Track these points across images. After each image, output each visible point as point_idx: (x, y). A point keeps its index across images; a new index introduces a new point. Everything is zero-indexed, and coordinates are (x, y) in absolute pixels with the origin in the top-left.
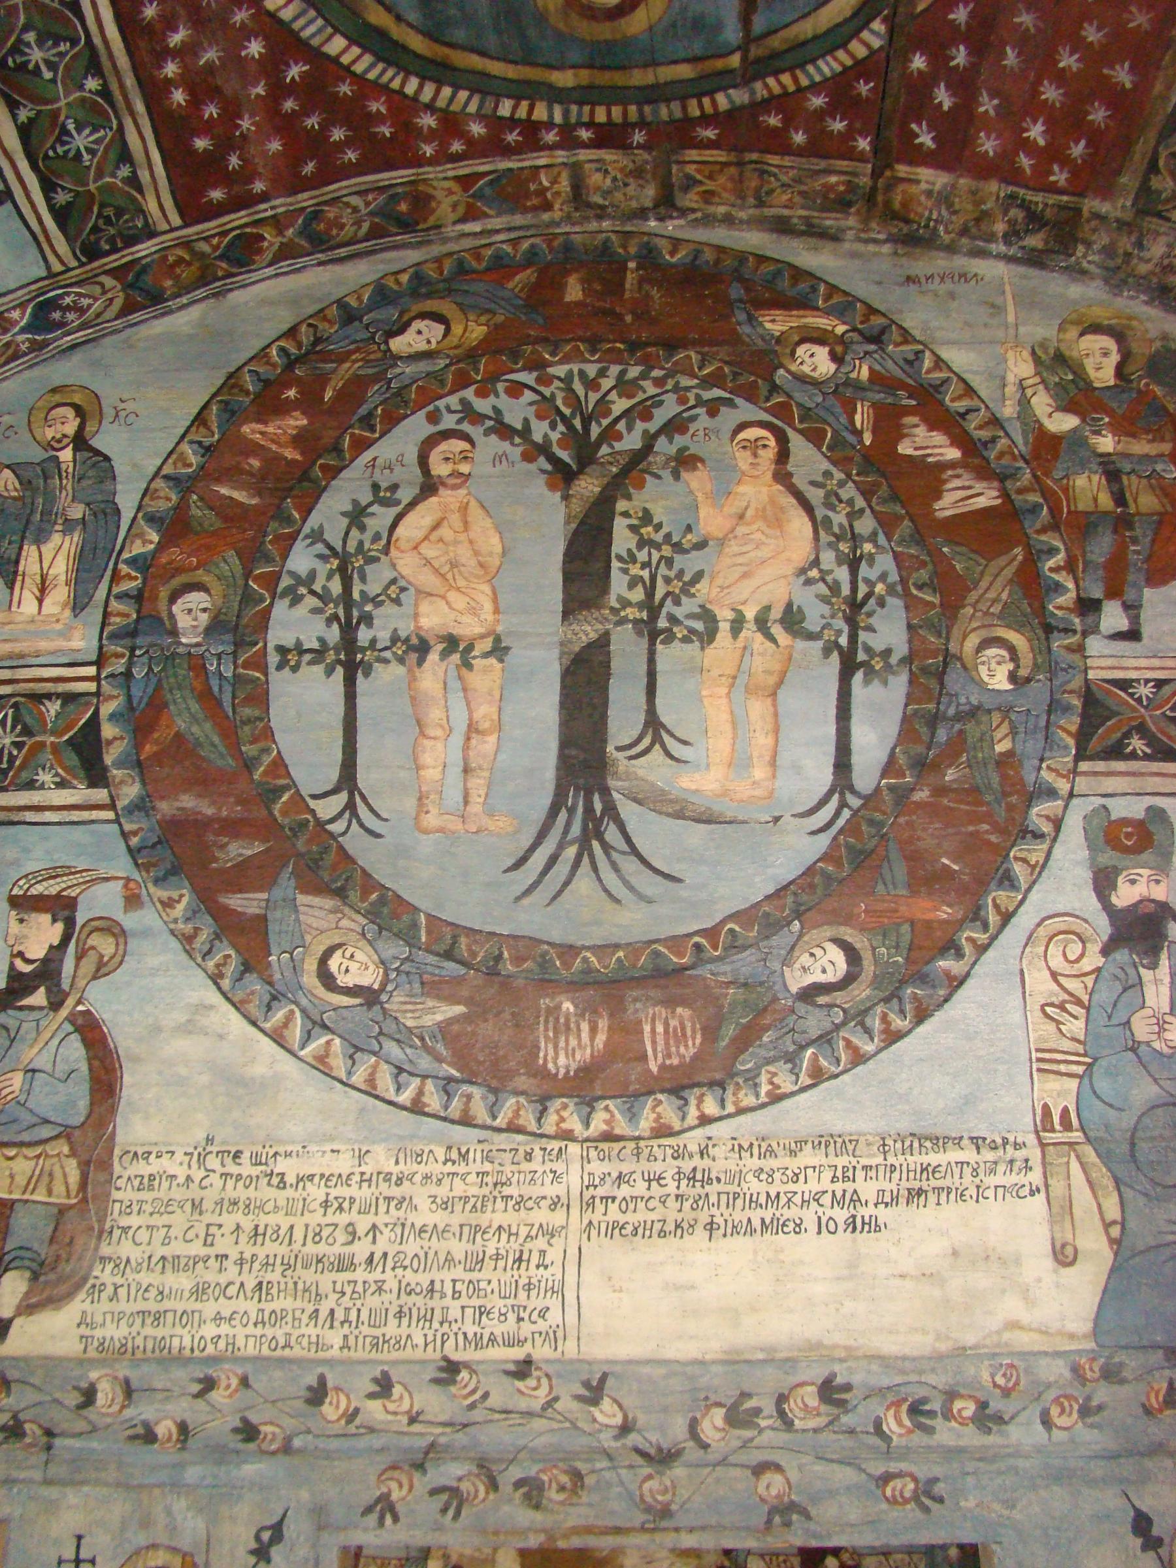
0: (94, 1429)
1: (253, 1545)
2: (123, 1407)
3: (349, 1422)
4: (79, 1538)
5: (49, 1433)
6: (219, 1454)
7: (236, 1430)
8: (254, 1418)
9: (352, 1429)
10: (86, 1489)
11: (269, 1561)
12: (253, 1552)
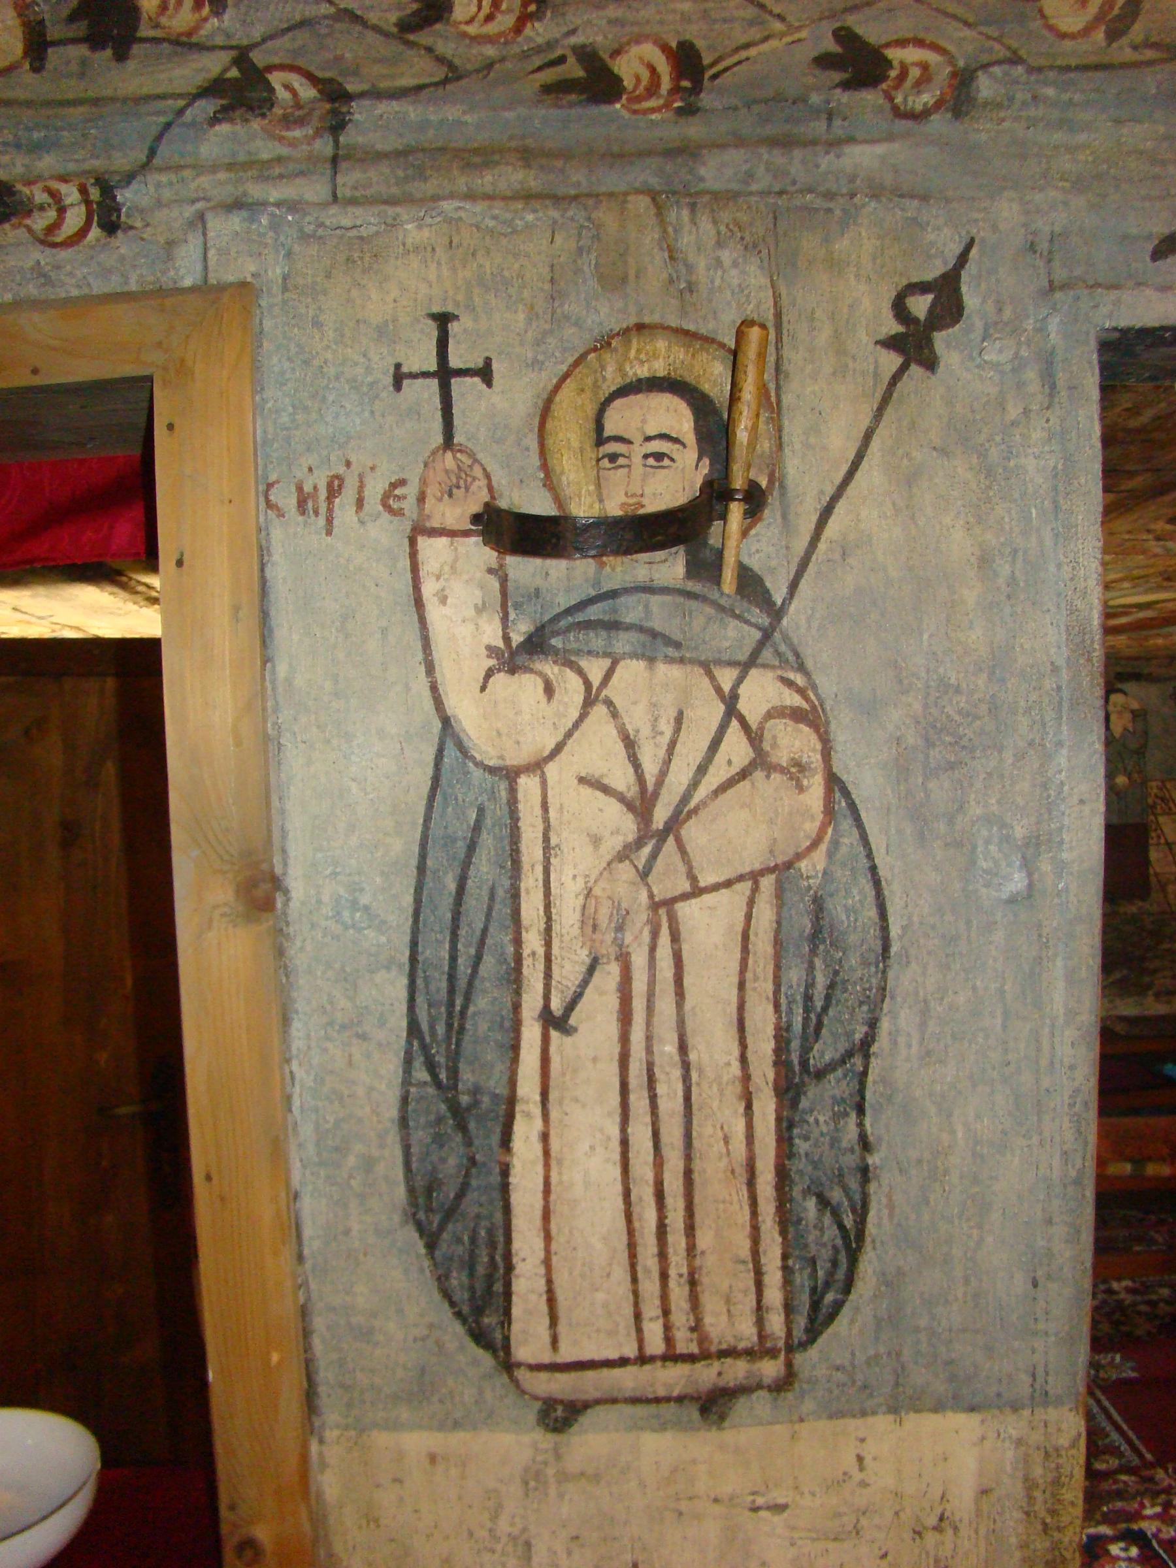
0: (453, 74)
1: (894, 327)
2: (523, 20)
3: (1113, 35)
4: (443, 320)
5: (335, 95)
6: (781, 122)
7: (824, 61)
8: (871, 30)
9: (1123, 51)
10: (447, 206)
11: (930, 364)
12: (892, 343)
